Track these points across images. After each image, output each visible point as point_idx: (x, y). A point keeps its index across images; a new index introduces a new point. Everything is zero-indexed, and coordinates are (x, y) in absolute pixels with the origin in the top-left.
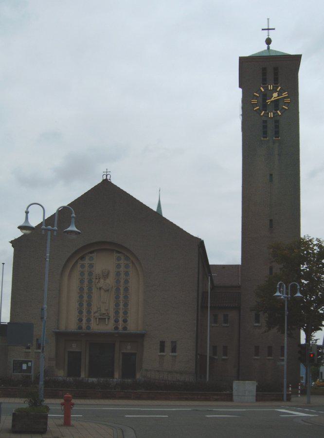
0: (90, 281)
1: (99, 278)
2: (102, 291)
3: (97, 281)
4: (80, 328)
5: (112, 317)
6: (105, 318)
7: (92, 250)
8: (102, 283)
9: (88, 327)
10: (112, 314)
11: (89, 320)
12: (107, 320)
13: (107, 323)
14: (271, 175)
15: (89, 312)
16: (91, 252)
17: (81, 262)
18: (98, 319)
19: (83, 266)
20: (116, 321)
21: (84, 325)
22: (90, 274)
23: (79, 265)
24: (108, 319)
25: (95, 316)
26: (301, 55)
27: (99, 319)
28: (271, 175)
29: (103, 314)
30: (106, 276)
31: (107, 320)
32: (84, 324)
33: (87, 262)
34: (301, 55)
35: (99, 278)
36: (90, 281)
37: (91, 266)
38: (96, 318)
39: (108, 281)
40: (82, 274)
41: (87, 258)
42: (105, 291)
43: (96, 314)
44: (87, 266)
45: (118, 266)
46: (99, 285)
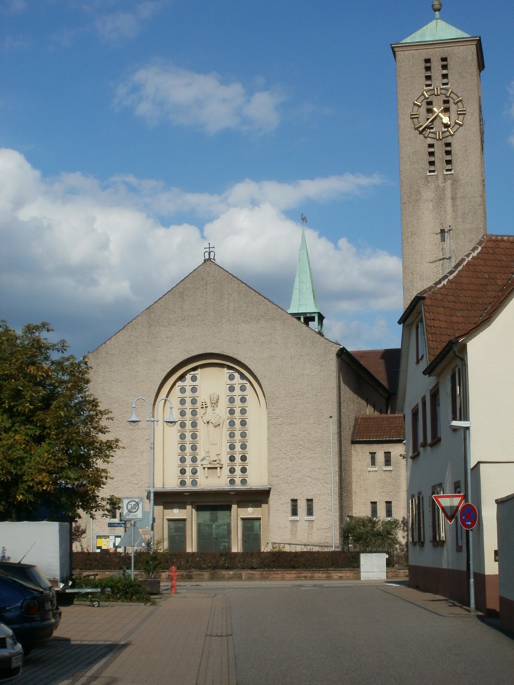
0: (194, 413)
2: (211, 425)
4: (183, 483)
6: (216, 468)
8: (210, 414)
9: (194, 483)
12: (218, 468)
16: (195, 369)
17: (179, 383)
18: (206, 469)
19: (183, 390)
20: (232, 471)
21: (188, 481)
22: (194, 401)
24: (221, 468)
25: (202, 465)
27: (209, 468)
29: (214, 461)
31: (218, 468)
32: (188, 478)
35: (206, 407)
36: (194, 413)
37: (194, 390)
39: (218, 410)
40: (183, 402)
41: (188, 377)
43: (204, 462)
44: (188, 389)
45: (232, 389)
46: (206, 418)
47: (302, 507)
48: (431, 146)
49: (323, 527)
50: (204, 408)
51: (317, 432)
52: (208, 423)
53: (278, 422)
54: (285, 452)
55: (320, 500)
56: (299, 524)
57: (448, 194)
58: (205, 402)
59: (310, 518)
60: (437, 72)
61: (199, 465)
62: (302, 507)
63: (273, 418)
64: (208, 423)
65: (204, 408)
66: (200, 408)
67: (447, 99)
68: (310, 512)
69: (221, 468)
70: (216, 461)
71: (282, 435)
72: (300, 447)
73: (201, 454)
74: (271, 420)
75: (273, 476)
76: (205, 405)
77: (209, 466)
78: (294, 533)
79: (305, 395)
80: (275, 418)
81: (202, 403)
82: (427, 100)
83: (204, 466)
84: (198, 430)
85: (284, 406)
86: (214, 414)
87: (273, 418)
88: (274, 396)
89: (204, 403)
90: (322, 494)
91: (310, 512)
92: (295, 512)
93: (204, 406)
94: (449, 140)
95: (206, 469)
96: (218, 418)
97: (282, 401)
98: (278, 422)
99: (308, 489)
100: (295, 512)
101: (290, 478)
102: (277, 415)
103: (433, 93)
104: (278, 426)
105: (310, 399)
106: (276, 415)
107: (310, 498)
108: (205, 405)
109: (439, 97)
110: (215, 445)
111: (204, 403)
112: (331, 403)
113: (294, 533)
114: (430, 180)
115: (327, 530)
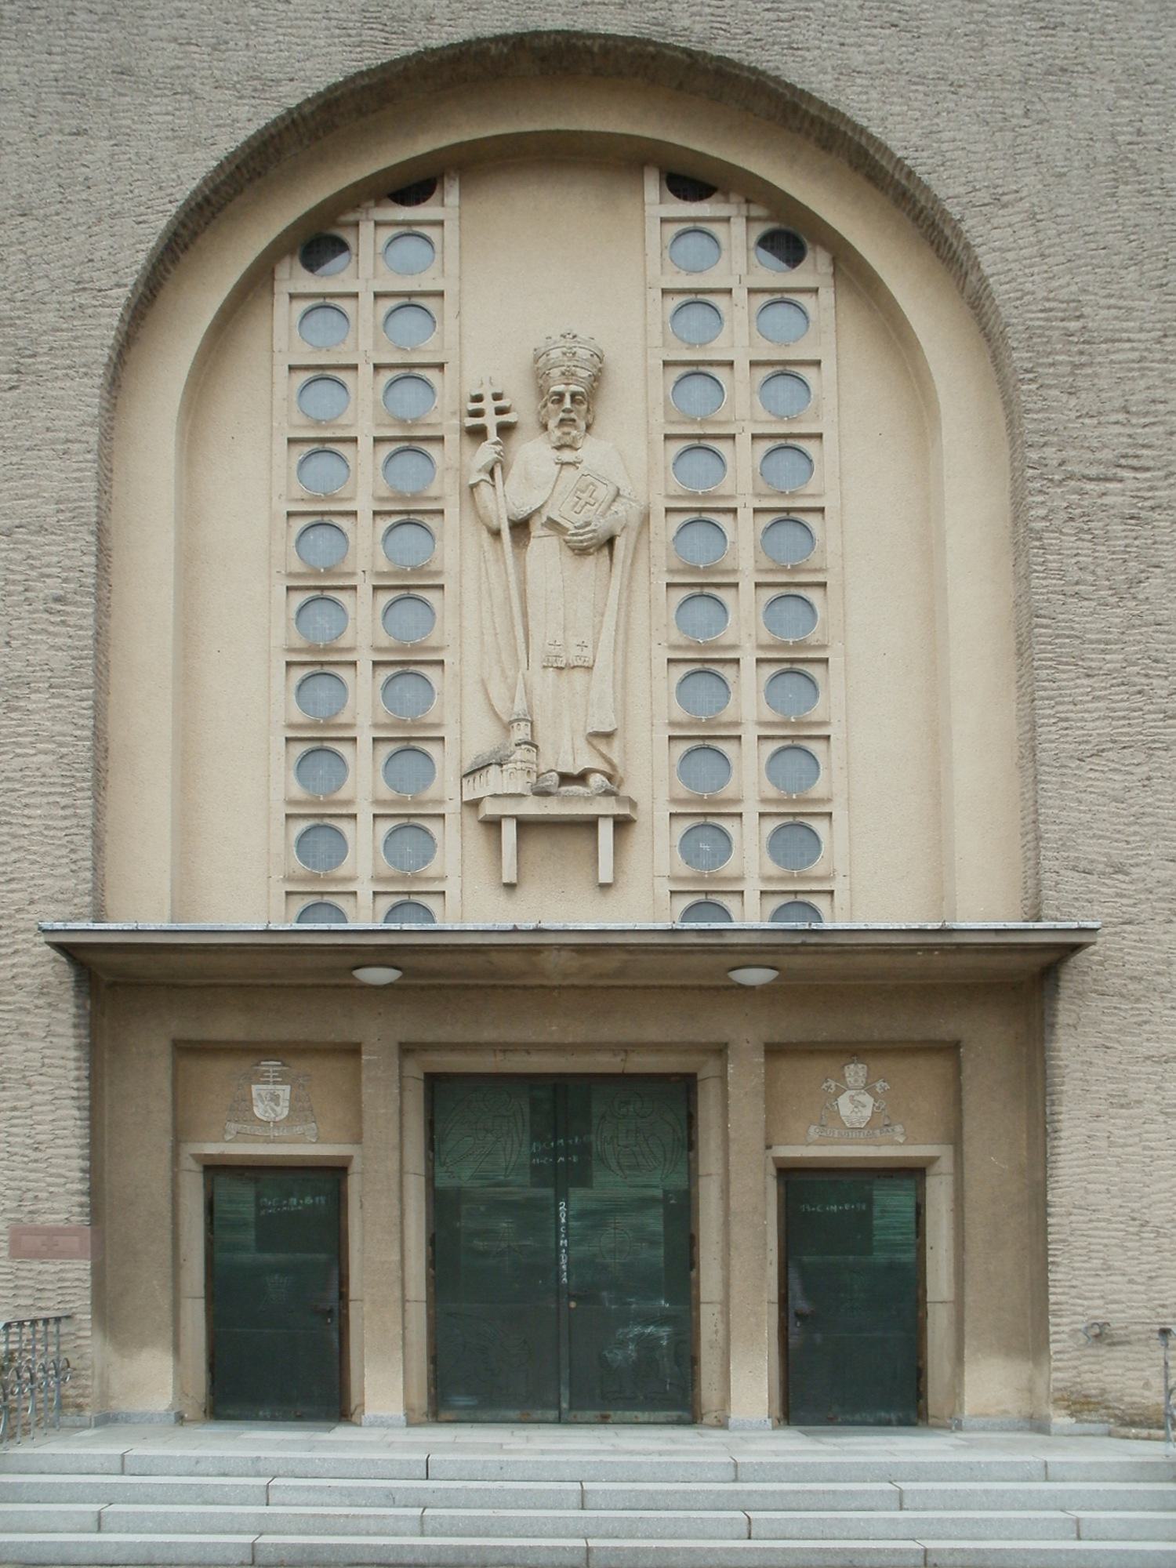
1: (505, 430)
2: (542, 546)
3: (487, 452)
5: (664, 810)
6: (590, 825)
7: (424, 144)
12: (606, 830)
13: (605, 875)
18: (509, 830)
24: (622, 824)
25: (475, 804)
27: (525, 825)
29: (565, 778)
31: (606, 830)
35: (505, 430)
38: (493, 825)
39: (592, 451)
42: (582, 552)
43: (494, 781)
52: (521, 527)
53: (1106, 500)
58: (497, 397)
61: (451, 809)
63: (1070, 477)
64: (521, 527)
66: (453, 438)
69: (622, 824)
70: (582, 778)
71: (1148, 589)
75: (1083, 865)
76: (500, 411)
77: (532, 808)
80: (1093, 471)
81: (478, 399)
83: (490, 809)
84: (438, 573)
85: (1159, 394)
86: (569, 472)
87: (1070, 477)
88: (1074, 325)
89: (488, 398)
93: (490, 421)
96: (604, 493)
97: (1141, 360)
98: (1106, 500)
102: (1106, 455)
104: (1117, 528)
106: (1098, 455)
108: (500, 411)
111: (488, 398)
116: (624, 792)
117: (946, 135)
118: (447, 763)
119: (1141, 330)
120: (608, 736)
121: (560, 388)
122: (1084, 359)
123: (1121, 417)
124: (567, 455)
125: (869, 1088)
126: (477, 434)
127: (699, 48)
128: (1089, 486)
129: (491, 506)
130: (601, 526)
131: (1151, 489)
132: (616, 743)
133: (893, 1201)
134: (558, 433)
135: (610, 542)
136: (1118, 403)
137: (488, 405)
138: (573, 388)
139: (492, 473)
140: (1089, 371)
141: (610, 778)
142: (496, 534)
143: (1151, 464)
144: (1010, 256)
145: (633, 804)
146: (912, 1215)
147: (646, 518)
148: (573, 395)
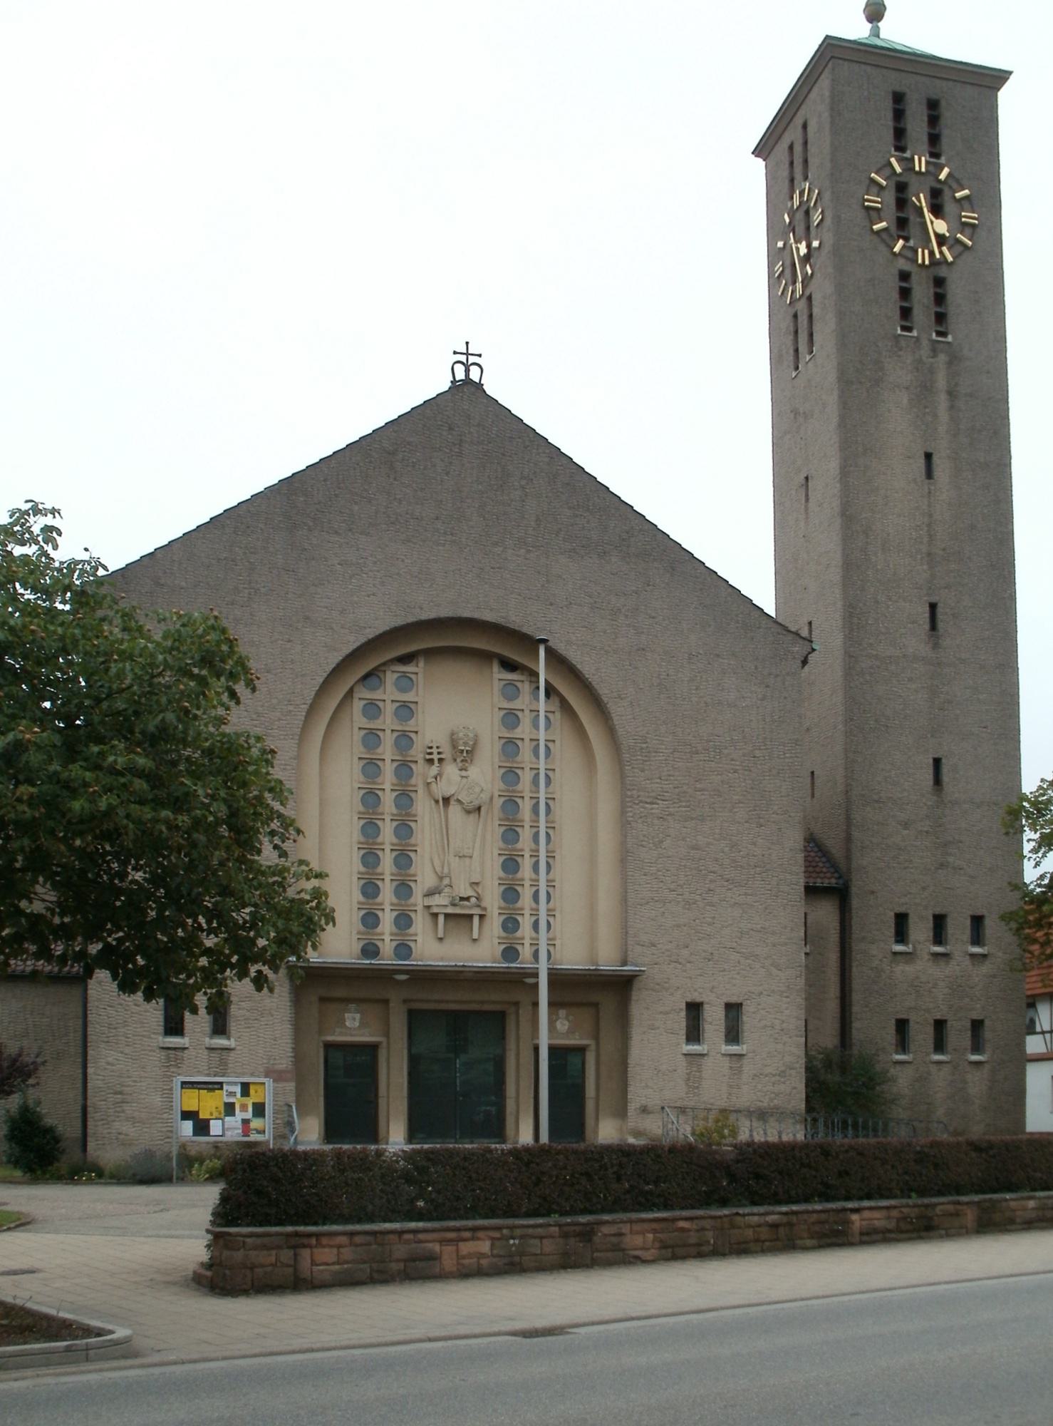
0: (404, 769)
1: (440, 760)
2: (454, 810)
3: (434, 770)
4: (370, 950)
5: (496, 912)
6: (470, 917)
8: (451, 779)
9: (403, 949)
10: (493, 900)
11: (404, 920)
12: (476, 920)
13: (475, 936)
14: (928, 456)
15: (404, 889)
16: (406, 659)
17: (363, 693)
18: (441, 919)
19: (372, 709)
21: (387, 947)
22: (404, 740)
23: (358, 705)
24: (482, 917)
25: (428, 907)
26: (1010, 73)
27: (447, 916)
28: (928, 456)
29: (462, 899)
30: (465, 754)
32: (387, 938)
33: (388, 693)
34: (1010, 73)
35: (440, 760)
36: (404, 769)
37: (406, 710)
38: (435, 915)
39: (474, 772)
40: (372, 738)
41: (390, 677)
42: (468, 812)
44: (389, 709)
45: (511, 718)
46: (442, 789)
47: (714, 1019)
48: (905, 276)
49: (768, 1070)
50: (436, 761)
51: (754, 844)
53: (653, 811)
54: (672, 887)
55: (759, 1007)
56: (708, 1063)
57: (941, 381)
58: (438, 747)
59: (734, 1049)
60: (917, 126)
61: (419, 908)
62: (714, 1019)
63: (641, 802)
64: (446, 801)
65: (436, 761)
66: (421, 762)
67: (939, 186)
68: (733, 1035)
69: (482, 917)
70: (468, 899)
71: (665, 844)
72: (712, 876)
73: (424, 878)
74: (638, 804)
76: (439, 753)
77: (450, 910)
78: (693, 1082)
79: (726, 751)
80: (648, 800)
81: (431, 748)
82: (898, 179)
84: (415, 816)
85: (671, 773)
86: (465, 780)
87: (641, 802)
88: (644, 745)
90: (765, 993)
91: (733, 1035)
92: (694, 1034)
93: (435, 757)
94: (943, 272)
95: (441, 919)
96: (477, 790)
97: (666, 760)
98: (653, 811)
99: (732, 978)
100: (694, 1034)
101: (685, 952)
103: (910, 165)
104: (656, 821)
105: (738, 763)
106: (651, 795)
107: (734, 1000)
108: (439, 753)
109: (922, 178)
110: (467, 860)
112: (789, 777)
113: (693, 1082)
114: (904, 345)
115: (777, 1078)
116: (483, 904)
117: (604, 670)
118: (418, 890)
119: (666, 749)
120: (477, 884)
121: (463, 748)
122: (646, 759)
123: (658, 781)
124: (464, 773)
125: (567, 1018)
126: (431, 761)
127: (517, 628)
128: (647, 806)
129: (436, 791)
130: (476, 803)
131: (668, 808)
132: (480, 887)
133: (574, 1060)
134: (460, 765)
135: (479, 809)
136: (658, 776)
137: (435, 751)
138: (467, 748)
139: (436, 779)
140: (648, 763)
141: (477, 898)
142: (437, 802)
143: (667, 798)
144: (623, 718)
145: (485, 909)
146: (580, 1066)
147: (492, 798)
148: (467, 751)
